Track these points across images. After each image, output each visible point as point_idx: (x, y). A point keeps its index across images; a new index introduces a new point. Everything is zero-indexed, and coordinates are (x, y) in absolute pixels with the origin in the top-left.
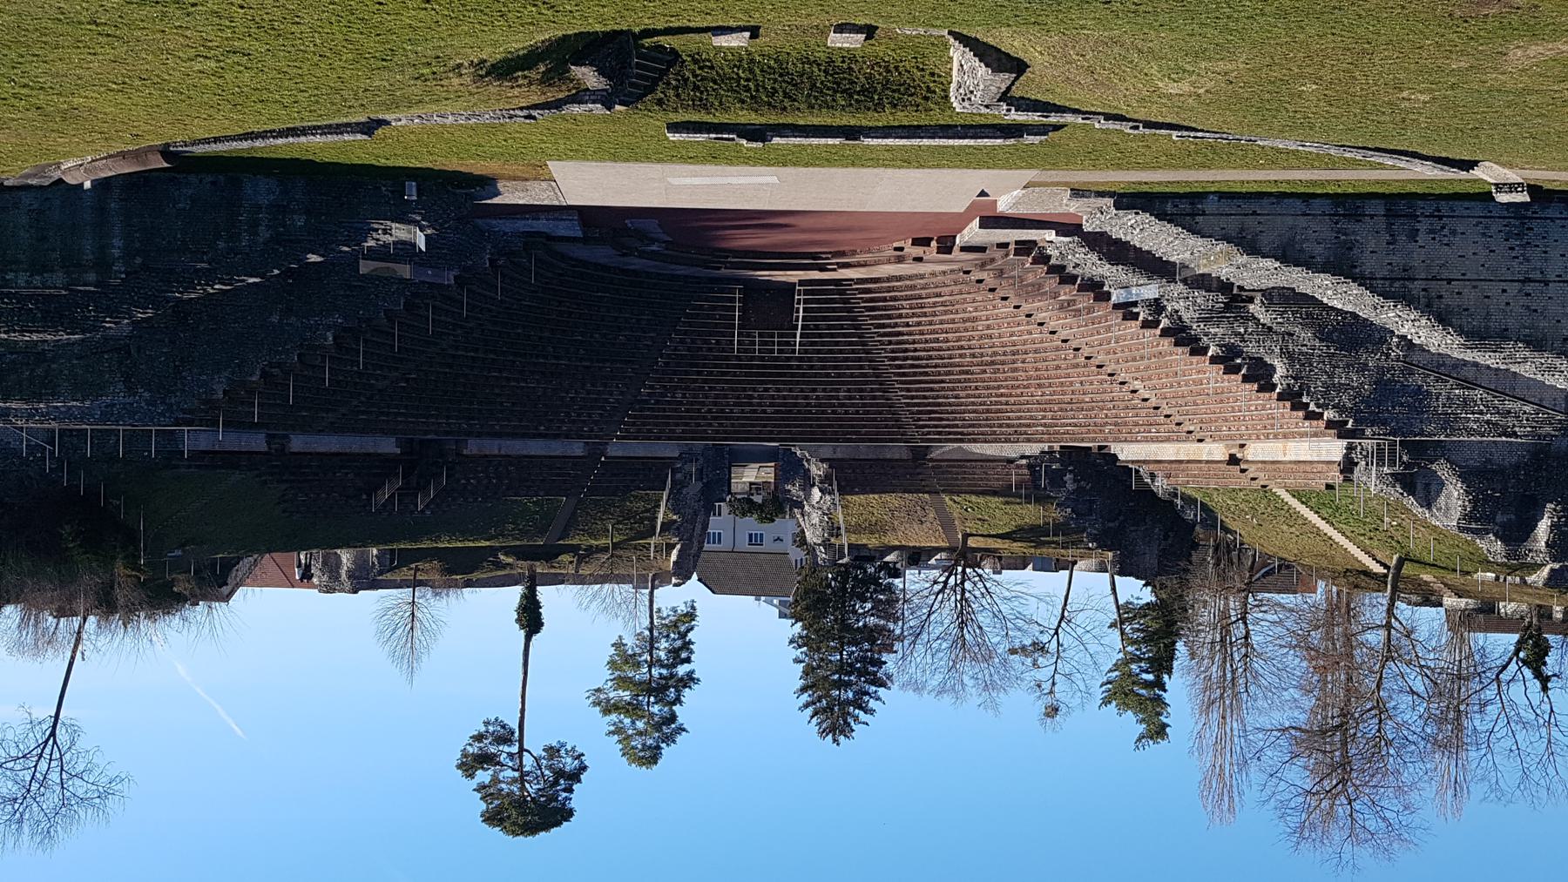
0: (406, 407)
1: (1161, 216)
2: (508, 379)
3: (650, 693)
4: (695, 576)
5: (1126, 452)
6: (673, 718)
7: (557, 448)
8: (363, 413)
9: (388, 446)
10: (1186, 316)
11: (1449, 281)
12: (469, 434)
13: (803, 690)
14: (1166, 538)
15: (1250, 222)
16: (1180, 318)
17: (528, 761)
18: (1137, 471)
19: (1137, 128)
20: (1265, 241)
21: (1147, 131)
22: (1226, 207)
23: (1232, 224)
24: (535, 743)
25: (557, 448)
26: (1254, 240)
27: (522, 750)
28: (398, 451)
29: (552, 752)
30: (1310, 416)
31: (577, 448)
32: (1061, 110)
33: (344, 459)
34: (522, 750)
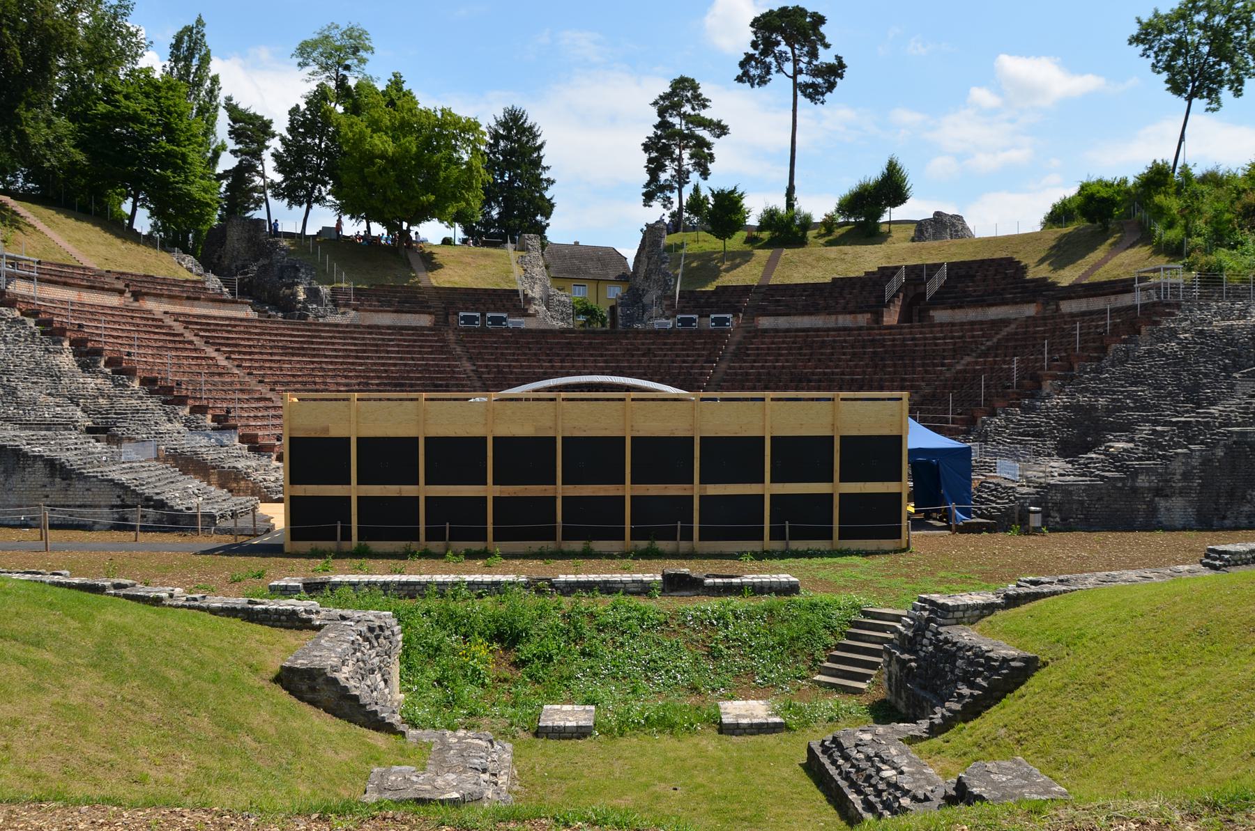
0: (936, 345)
1: (161, 505)
2: (843, 374)
3: (679, 132)
4: (631, 262)
5: (247, 312)
6: (661, 113)
7: (782, 322)
8: (978, 336)
9: (941, 316)
10: (160, 416)
12: (868, 329)
13: (541, 147)
14: (220, 257)
15: (58, 498)
16: (166, 413)
17: (788, 67)
18: (233, 294)
19: (118, 586)
20: (39, 474)
21: (100, 582)
22: (87, 515)
23: (78, 493)
24: (780, 84)
25: (782, 322)
26: (52, 475)
27: (794, 78)
28: (932, 313)
29: (763, 81)
30: (34, 314)
31: (765, 322)
32: (230, 612)
33: (981, 302)
34: (794, 78)
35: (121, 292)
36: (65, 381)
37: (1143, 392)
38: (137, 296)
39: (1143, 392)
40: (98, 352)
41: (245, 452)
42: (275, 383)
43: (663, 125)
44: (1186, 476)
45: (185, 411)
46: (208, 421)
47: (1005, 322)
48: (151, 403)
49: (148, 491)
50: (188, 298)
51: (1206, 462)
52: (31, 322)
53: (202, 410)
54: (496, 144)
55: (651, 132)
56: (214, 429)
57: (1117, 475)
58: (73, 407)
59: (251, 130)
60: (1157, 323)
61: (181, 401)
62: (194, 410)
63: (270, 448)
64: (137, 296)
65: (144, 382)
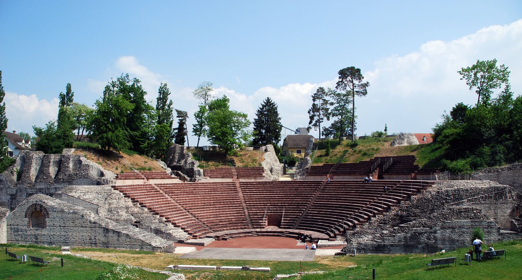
5: (177, 181)
6: (314, 100)
11: (82, 227)
27: (353, 89)
35: (143, 179)
36: (130, 209)
37: (417, 211)
38: (148, 179)
39: (417, 211)
40: (138, 201)
41: (173, 228)
42: (183, 205)
43: (314, 105)
44: (400, 241)
45: (158, 217)
46: (164, 219)
47: (395, 183)
48: (150, 215)
49: (147, 242)
50: (161, 178)
51: (405, 237)
52: (122, 194)
53: (163, 216)
54: (263, 108)
55: (311, 107)
56: (165, 221)
57: (380, 241)
58: (131, 216)
59: (182, 115)
60: (426, 189)
61: (157, 214)
62: (161, 216)
63: (179, 226)
64: (148, 179)
65: (149, 209)
